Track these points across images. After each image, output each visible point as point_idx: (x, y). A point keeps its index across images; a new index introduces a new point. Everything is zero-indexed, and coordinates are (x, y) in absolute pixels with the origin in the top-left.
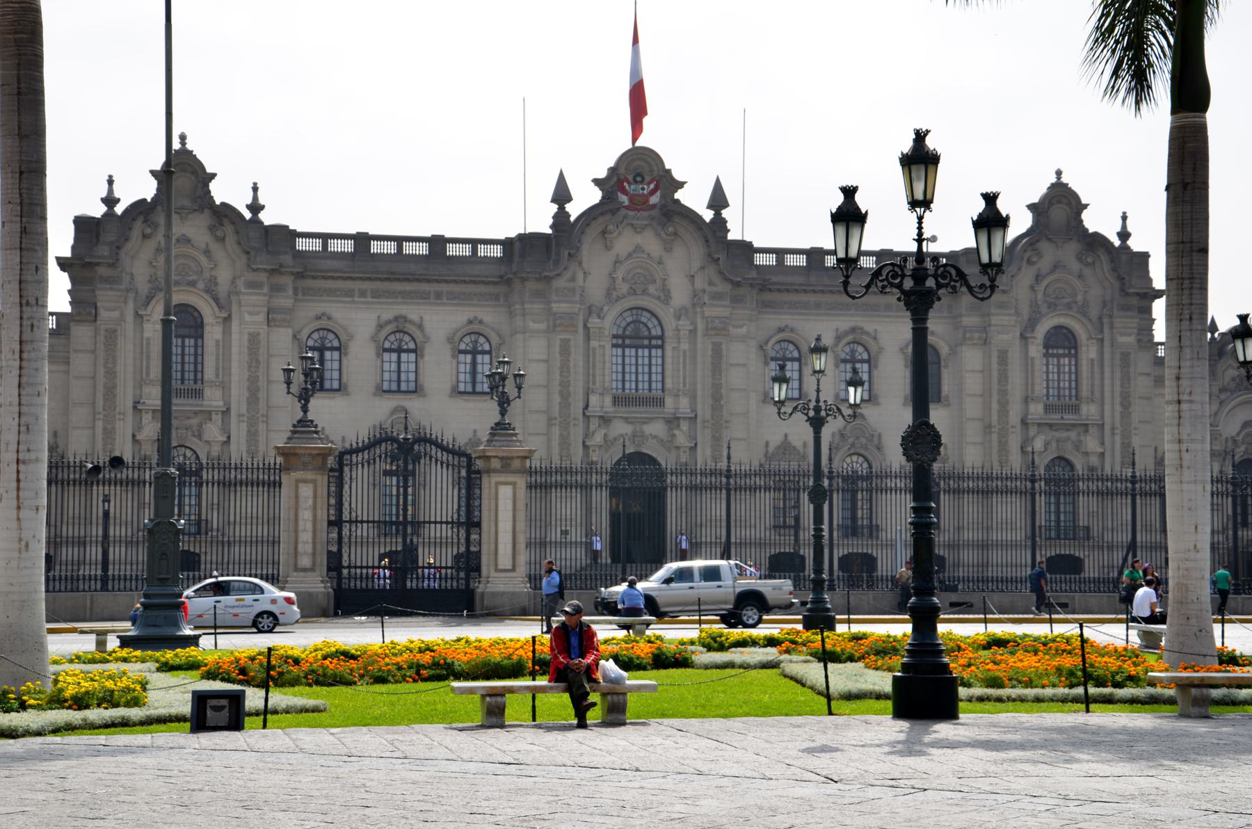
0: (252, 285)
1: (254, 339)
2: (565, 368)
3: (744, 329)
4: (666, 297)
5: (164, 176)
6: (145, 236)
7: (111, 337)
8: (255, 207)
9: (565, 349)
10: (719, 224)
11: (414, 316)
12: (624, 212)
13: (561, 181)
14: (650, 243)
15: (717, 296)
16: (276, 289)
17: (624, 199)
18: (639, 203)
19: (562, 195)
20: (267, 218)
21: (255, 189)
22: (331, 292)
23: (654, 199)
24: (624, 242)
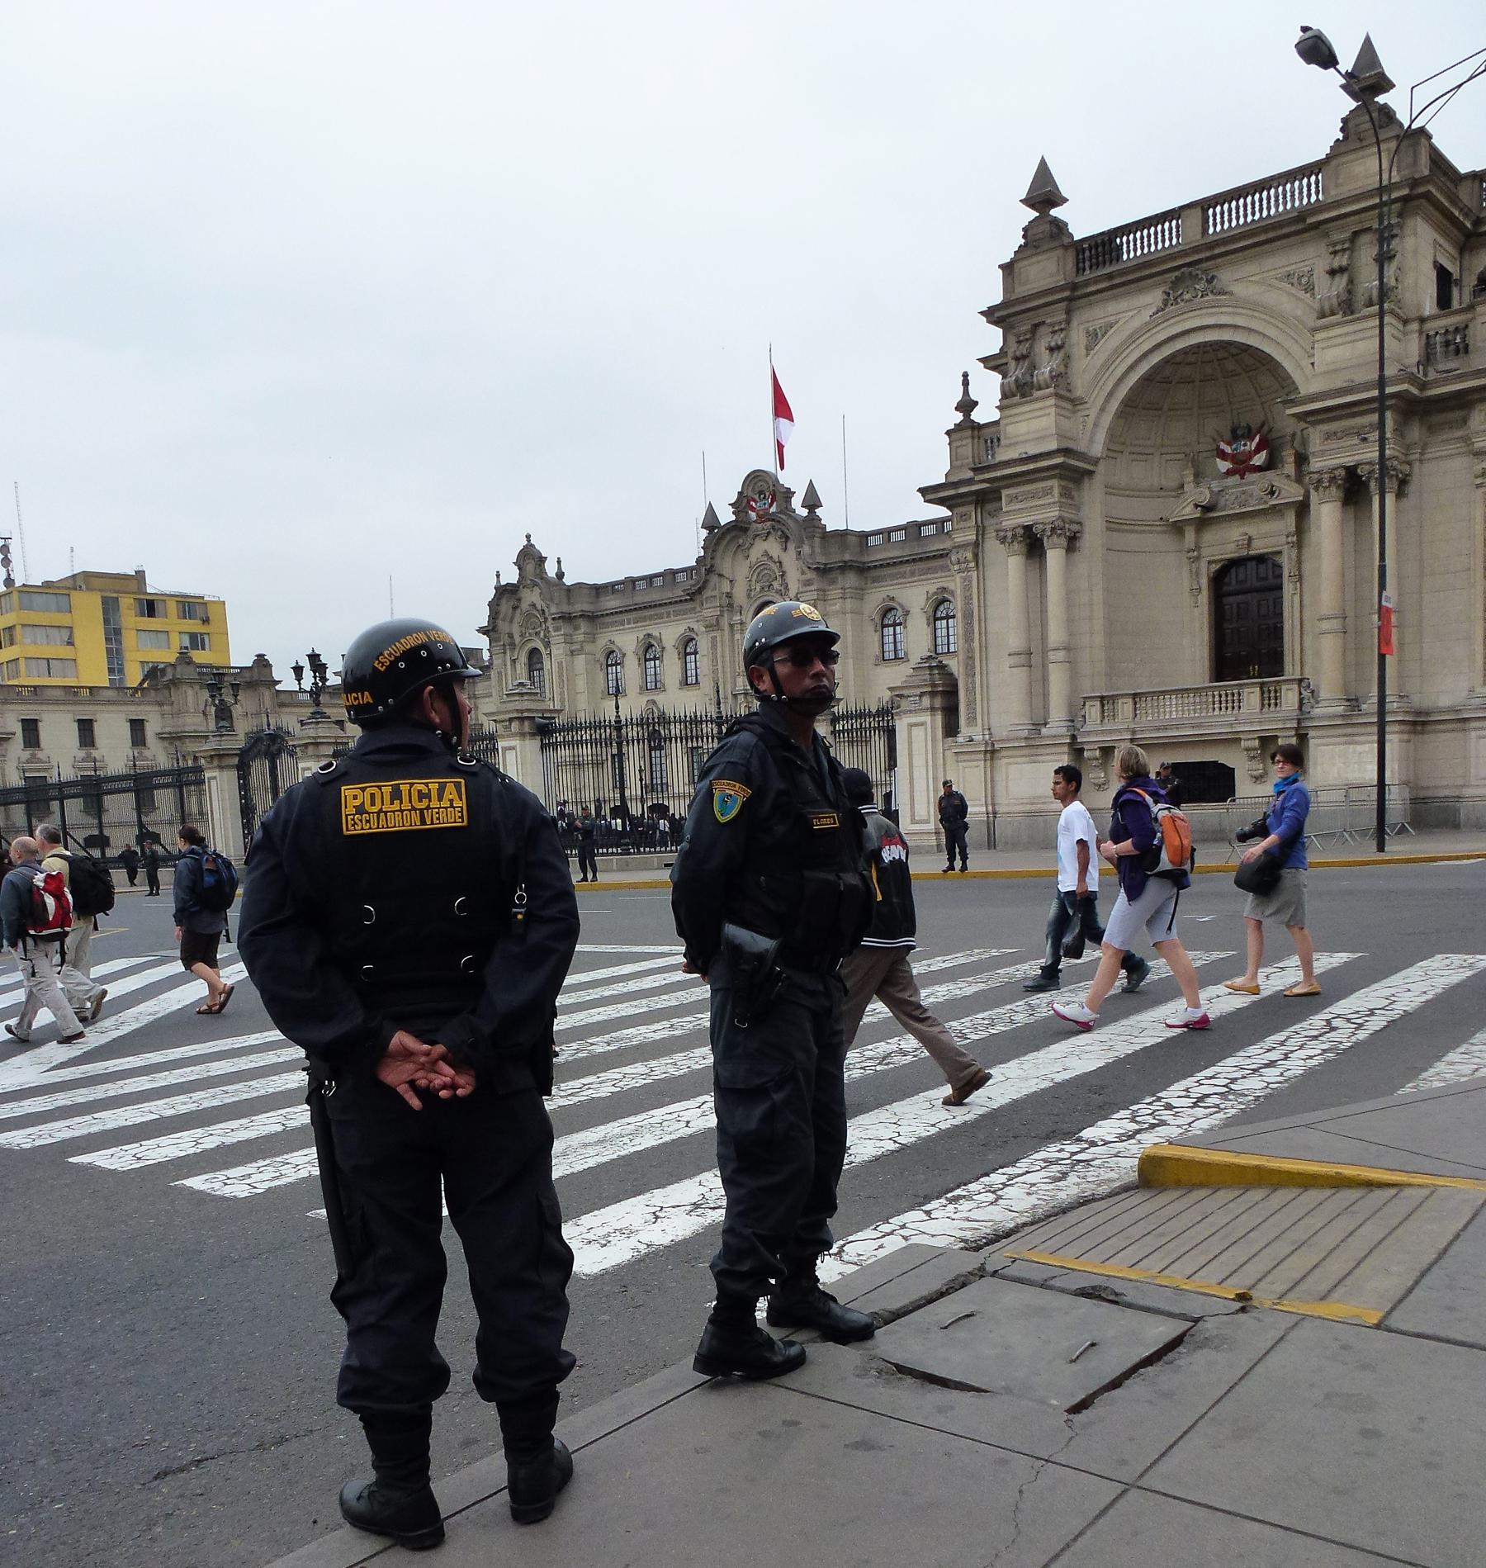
0: (557, 629)
1: (560, 664)
2: (714, 659)
3: (838, 607)
4: (786, 588)
5: (520, 563)
6: (515, 608)
7: (500, 673)
8: (560, 575)
9: (714, 646)
10: (813, 521)
11: (656, 633)
12: (755, 526)
13: (711, 511)
14: (773, 547)
15: (808, 583)
16: (576, 628)
17: (753, 515)
18: (763, 517)
19: (710, 522)
20: (568, 580)
21: (559, 562)
22: (614, 624)
23: (773, 509)
24: (758, 549)
